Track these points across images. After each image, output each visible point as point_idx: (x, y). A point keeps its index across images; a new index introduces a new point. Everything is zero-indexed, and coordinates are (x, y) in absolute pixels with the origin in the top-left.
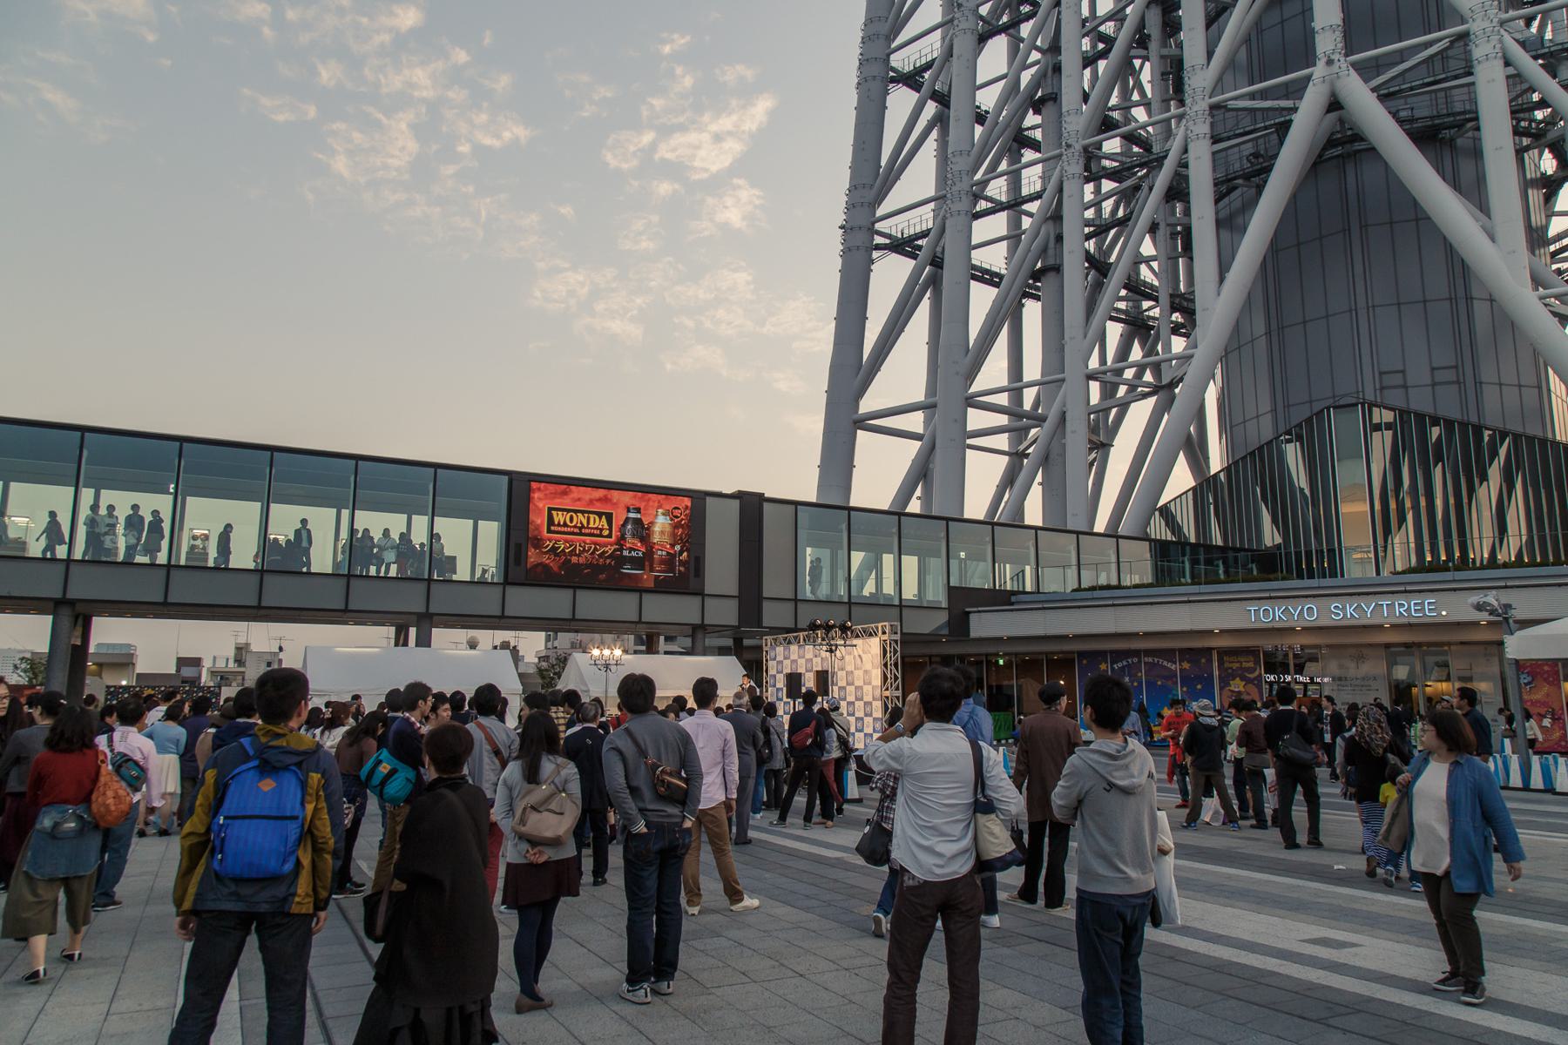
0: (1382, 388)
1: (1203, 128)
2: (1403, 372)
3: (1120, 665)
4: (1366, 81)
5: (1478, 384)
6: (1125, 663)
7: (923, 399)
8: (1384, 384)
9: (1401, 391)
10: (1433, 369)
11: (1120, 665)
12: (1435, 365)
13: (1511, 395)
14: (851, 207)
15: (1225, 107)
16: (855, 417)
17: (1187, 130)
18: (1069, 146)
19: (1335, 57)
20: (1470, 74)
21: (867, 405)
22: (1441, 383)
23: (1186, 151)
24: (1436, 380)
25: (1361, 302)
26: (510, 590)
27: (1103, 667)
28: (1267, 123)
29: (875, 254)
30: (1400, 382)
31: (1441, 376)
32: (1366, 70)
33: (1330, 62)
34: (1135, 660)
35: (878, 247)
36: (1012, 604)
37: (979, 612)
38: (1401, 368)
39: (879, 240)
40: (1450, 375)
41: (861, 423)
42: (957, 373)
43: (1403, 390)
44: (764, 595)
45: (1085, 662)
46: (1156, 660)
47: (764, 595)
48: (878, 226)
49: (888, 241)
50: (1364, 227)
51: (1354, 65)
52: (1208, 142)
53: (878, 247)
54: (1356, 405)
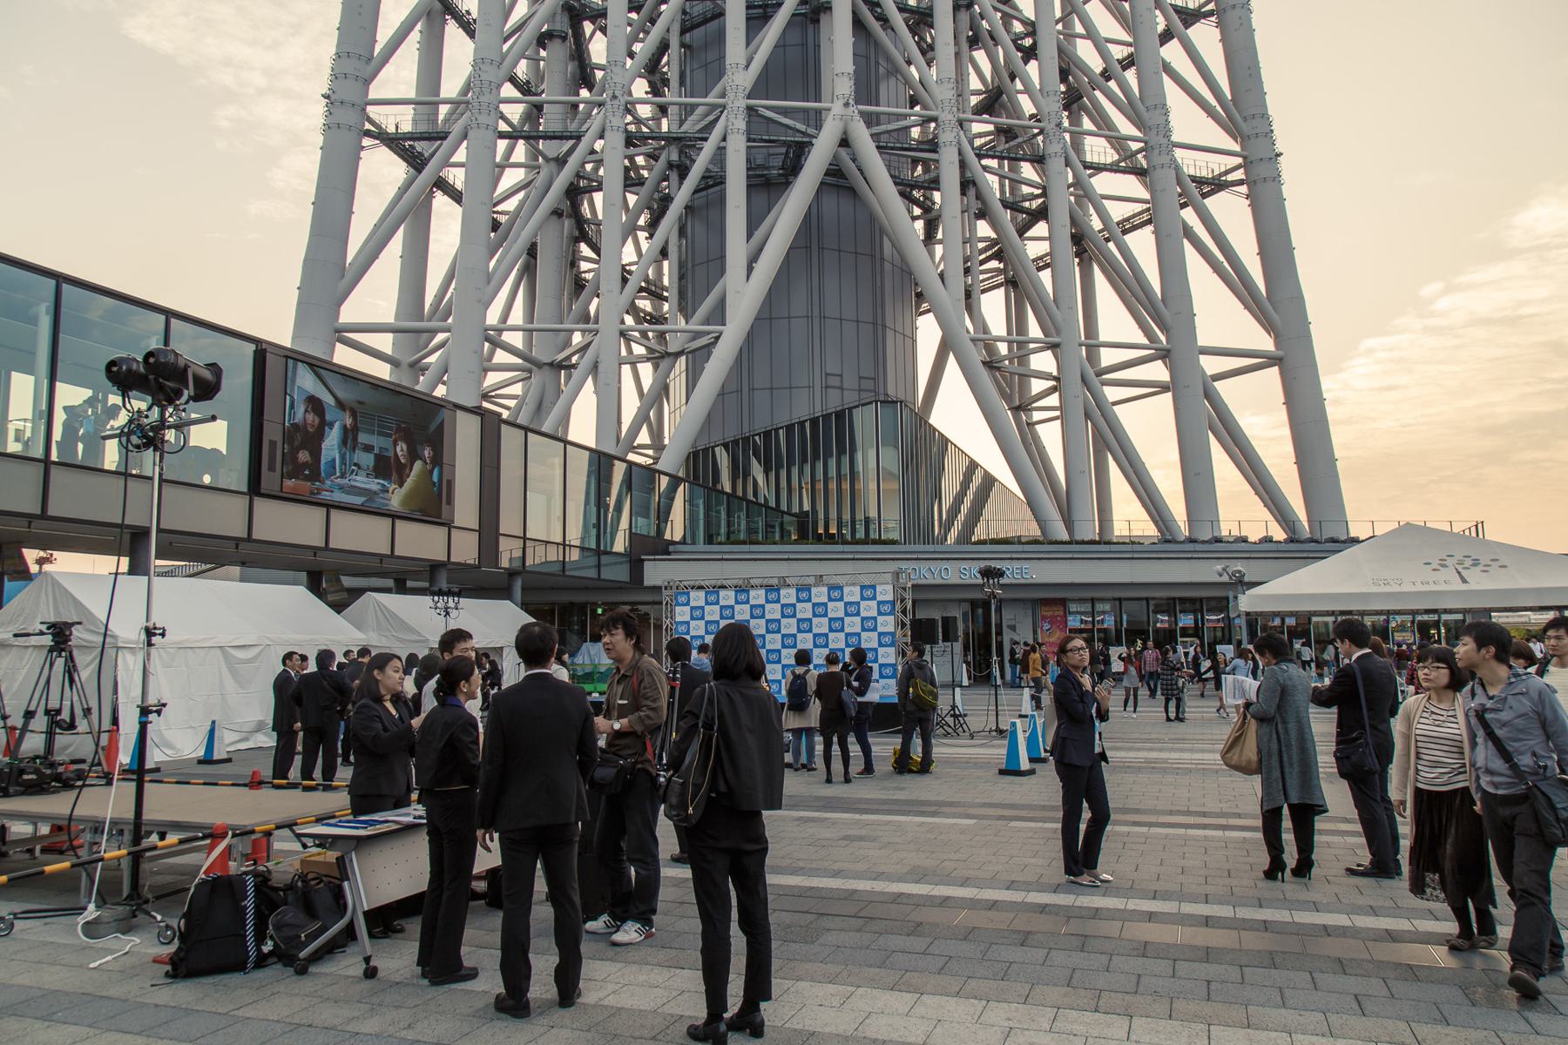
0: (827, 387)
1: (741, 124)
2: (841, 376)
4: (868, 128)
7: (392, 321)
8: (829, 384)
9: (838, 392)
10: (860, 378)
15: (757, 111)
16: (337, 325)
17: (727, 120)
18: (614, 97)
20: (935, 151)
21: (349, 313)
23: (724, 139)
24: (862, 387)
25: (816, 313)
28: (772, 138)
29: (366, 142)
30: (838, 384)
33: (847, 105)
35: (368, 134)
36: (669, 554)
37: (655, 560)
38: (840, 373)
39: (368, 126)
43: (840, 391)
50: (821, 248)
51: (861, 113)
52: (744, 138)
54: (896, 402)
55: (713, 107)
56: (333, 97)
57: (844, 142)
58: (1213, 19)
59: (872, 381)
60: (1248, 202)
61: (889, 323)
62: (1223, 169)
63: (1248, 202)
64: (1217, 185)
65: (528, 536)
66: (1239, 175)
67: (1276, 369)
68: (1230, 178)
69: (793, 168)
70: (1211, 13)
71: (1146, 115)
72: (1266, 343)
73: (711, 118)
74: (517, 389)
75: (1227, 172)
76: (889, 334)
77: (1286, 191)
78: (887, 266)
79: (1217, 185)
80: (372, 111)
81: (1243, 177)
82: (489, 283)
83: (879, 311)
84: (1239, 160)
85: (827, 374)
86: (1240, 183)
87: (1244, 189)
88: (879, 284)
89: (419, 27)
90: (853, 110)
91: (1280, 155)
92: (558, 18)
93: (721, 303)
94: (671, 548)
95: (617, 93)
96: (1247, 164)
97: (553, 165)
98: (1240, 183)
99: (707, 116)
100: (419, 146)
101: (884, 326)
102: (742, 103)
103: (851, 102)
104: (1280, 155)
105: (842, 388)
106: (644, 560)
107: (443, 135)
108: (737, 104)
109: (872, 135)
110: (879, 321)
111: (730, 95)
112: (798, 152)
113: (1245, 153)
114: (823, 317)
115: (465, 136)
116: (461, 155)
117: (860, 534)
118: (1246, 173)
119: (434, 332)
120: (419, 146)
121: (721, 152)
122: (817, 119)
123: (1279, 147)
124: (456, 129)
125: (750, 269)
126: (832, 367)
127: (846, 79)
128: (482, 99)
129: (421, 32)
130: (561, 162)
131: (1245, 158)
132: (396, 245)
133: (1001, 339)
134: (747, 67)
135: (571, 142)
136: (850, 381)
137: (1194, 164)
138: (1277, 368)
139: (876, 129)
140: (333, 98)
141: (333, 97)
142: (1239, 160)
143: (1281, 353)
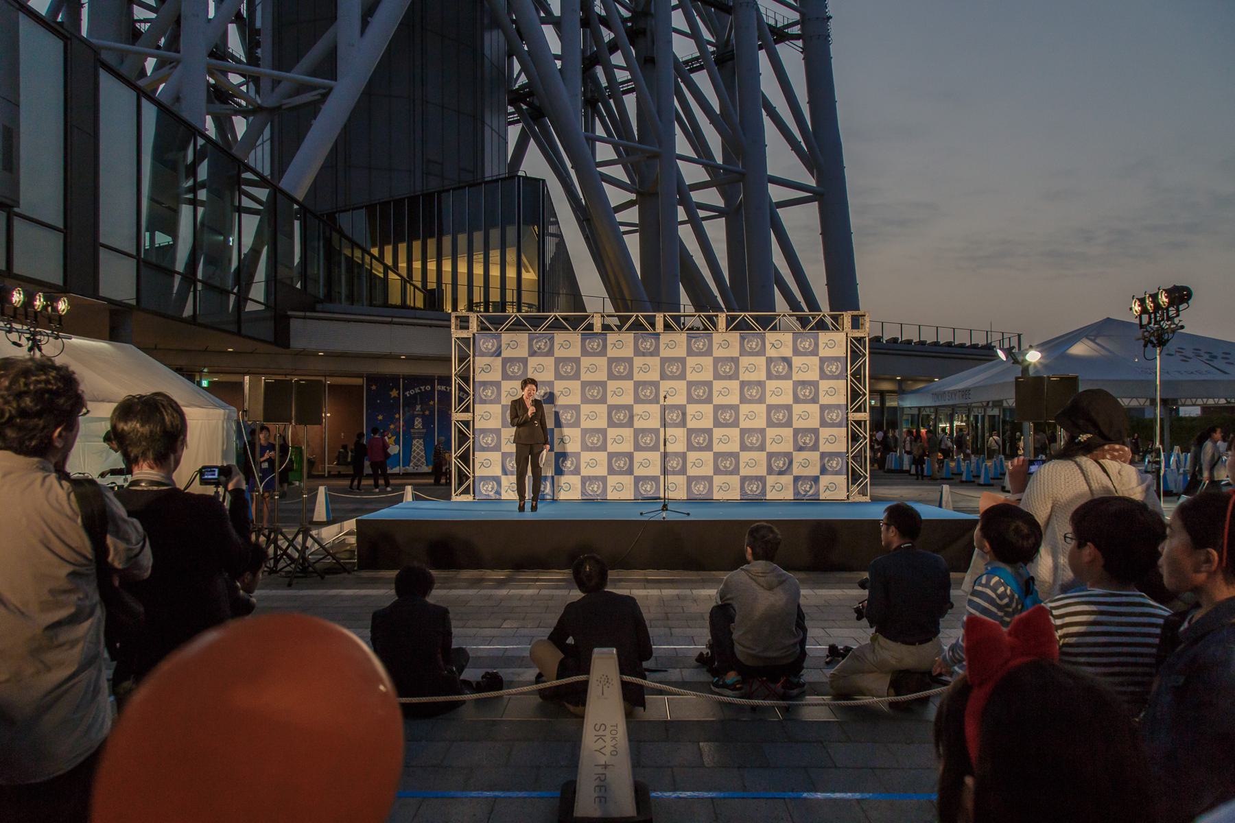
3: (412, 392)
6: (417, 390)
11: (412, 392)
27: (394, 393)
34: (428, 388)
45: (374, 388)
46: (422, 388)
60: (802, 56)
62: (786, 23)
64: (780, 35)
66: (796, 30)
68: (790, 31)
78: (486, 61)
79: (780, 35)
86: (797, 37)
87: (800, 43)
91: (830, 17)
96: (802, 22)
98: (797, 37)
104: (830, 17)
118: (802, 29)
125: (365, 24)
131: (802, 15)
133: (602, 140)
142: (796, 16)
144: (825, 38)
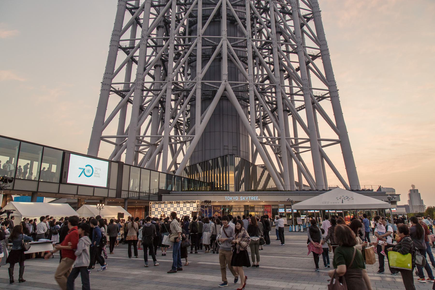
0: (224, 149)
1: (200, 87)
2: (228, 146)
5: (240, 151)
9: (227, 150)
10: (233, 147)
12: (233, 146)
13: (244, 153)
14: (105, 78)
17: (196, 86)
18: (169, 81)
19: (227, 81)
21: (104, 134)
22: (234, 150)
26: (61, 185)
29: (111, 93)
31: (234, 148)
32: (231, 84)
33: (225, 81)
35: (111, 91)
38: (227, 145)
39: (112, 89)
40: (235, 148)
41: (102, 138)
42: (135, 130)
44: (122, 189)
47: (122, 189)
48: (112, 85)
49: (114, 90)
51: (229, 83)
53: (111, 91)
55: (194, 83)
56: (103, 83)
57: (225, 90)
58: (320, 57)
59: (236, 147)
61: (241, 132)
62: (324, 94)
63: (331, 102)
64: (323, 98)
65: (129, 190)
66: (328, 95)
67: (339, 144)
68: (326, 96)
69: (214, 95)
70: (320, 56)
71: (302, 82)
72: (337, 137)
73: (193, 85)
74: (147, 150)
75: (325, 95)
76: (241, 135)
77: (340, 99)
79: (323, 98)
80: (112, 85)
81: (329, 96)
82: (138, 126)
83: (238, 130)
84: (328, 92)
85: (224, 146)
86: (328, 97)
87: (329, 99)
88: (238, 123)
89: (126, 65)
90: (227, 82)
92: (159, 62)
93: (194, 131)
94: (170, 192)
95: (170, 80)
97: (156, 96)
98: (328, 97)
99: (192, 84)
100: (124, 93)
101: (239, 133)
102: (200, 82)
103: (227, 81)
105: (228, 149)
106: (162, 195)
107: (129, 91)
108: (199, 82)
109: (232, 88)
110: (238, 132)
111: (197, 80)
112: (215, 92)
113: (329, 90)
114: (223, 132)
115: (134, 91)
116: (133, 95)
117: (224, 189)
119: (126, 138)
120: (124, 93)
121: (195, 92)
122: (219, 84)
123: (338, 88)
124: (132, 89)
125: (201, 121)
126: (226, 144)
127: (226, 75)
128: (138, 82)
129: (126, 66)
130: (158, 95)
131: (329, 91)
132: (118, 115)
134: (201, 73)
135: (160, 91)
136: (230, 147)
137: (316, 93)
138: (340, 144)
139: (233, 87)
140: (103, 83)
141: (103, 83)
142: (328, 92)
143: (340, 140)
144: (337, 96)
